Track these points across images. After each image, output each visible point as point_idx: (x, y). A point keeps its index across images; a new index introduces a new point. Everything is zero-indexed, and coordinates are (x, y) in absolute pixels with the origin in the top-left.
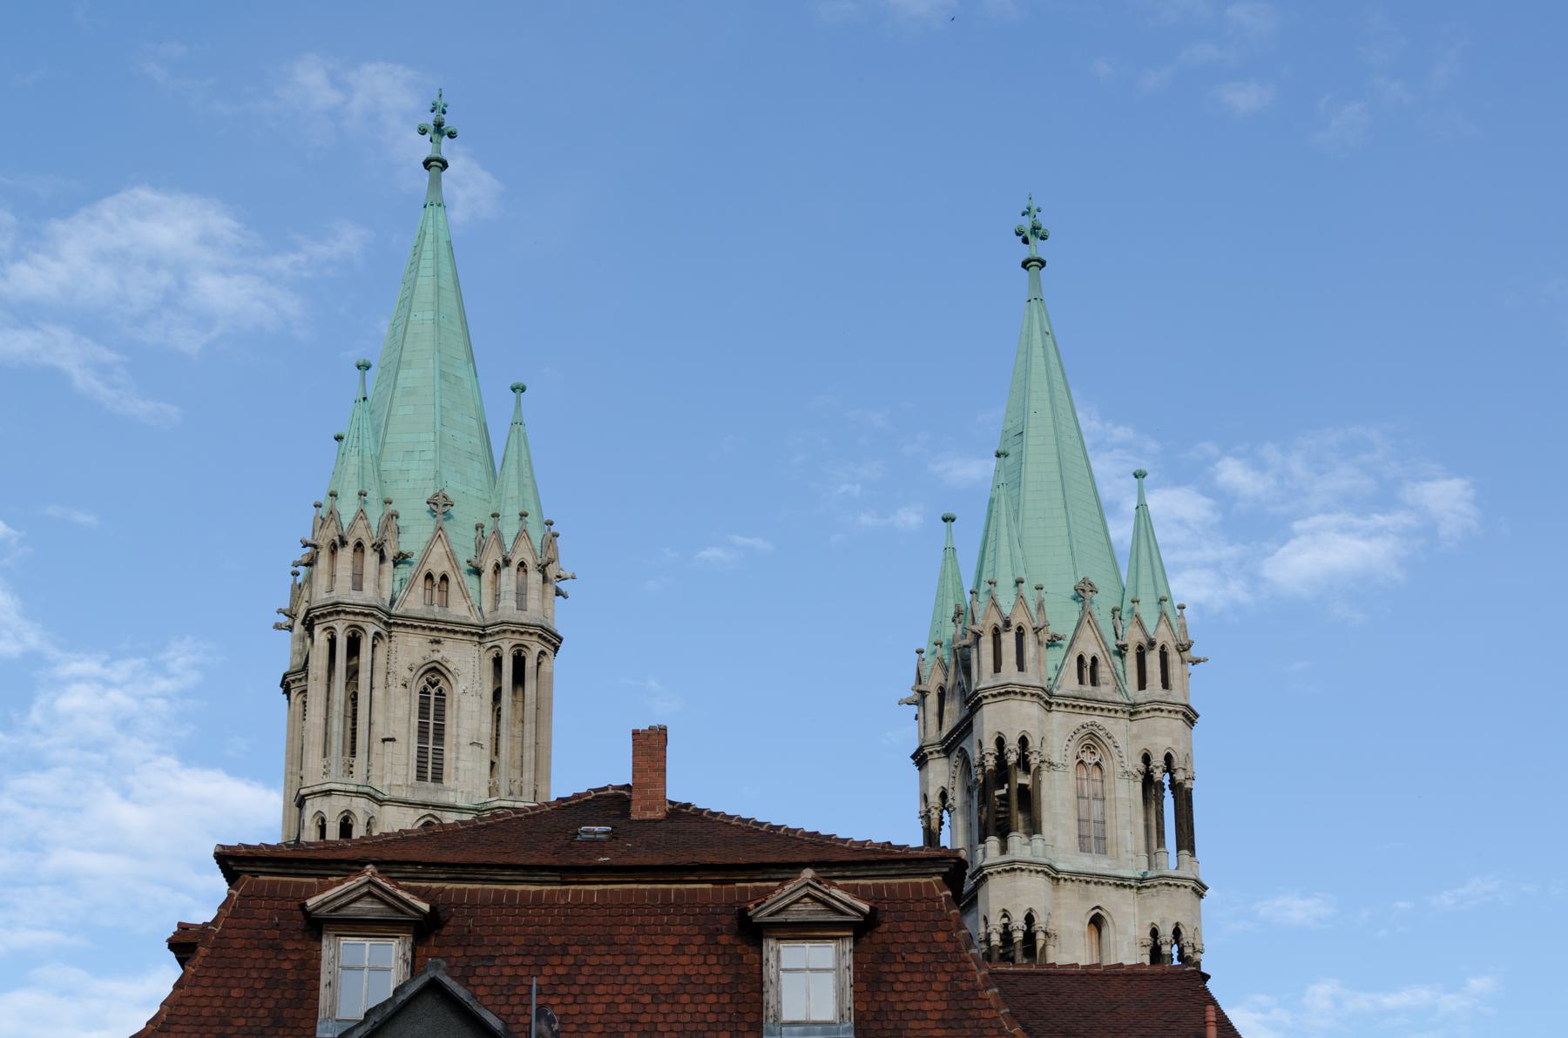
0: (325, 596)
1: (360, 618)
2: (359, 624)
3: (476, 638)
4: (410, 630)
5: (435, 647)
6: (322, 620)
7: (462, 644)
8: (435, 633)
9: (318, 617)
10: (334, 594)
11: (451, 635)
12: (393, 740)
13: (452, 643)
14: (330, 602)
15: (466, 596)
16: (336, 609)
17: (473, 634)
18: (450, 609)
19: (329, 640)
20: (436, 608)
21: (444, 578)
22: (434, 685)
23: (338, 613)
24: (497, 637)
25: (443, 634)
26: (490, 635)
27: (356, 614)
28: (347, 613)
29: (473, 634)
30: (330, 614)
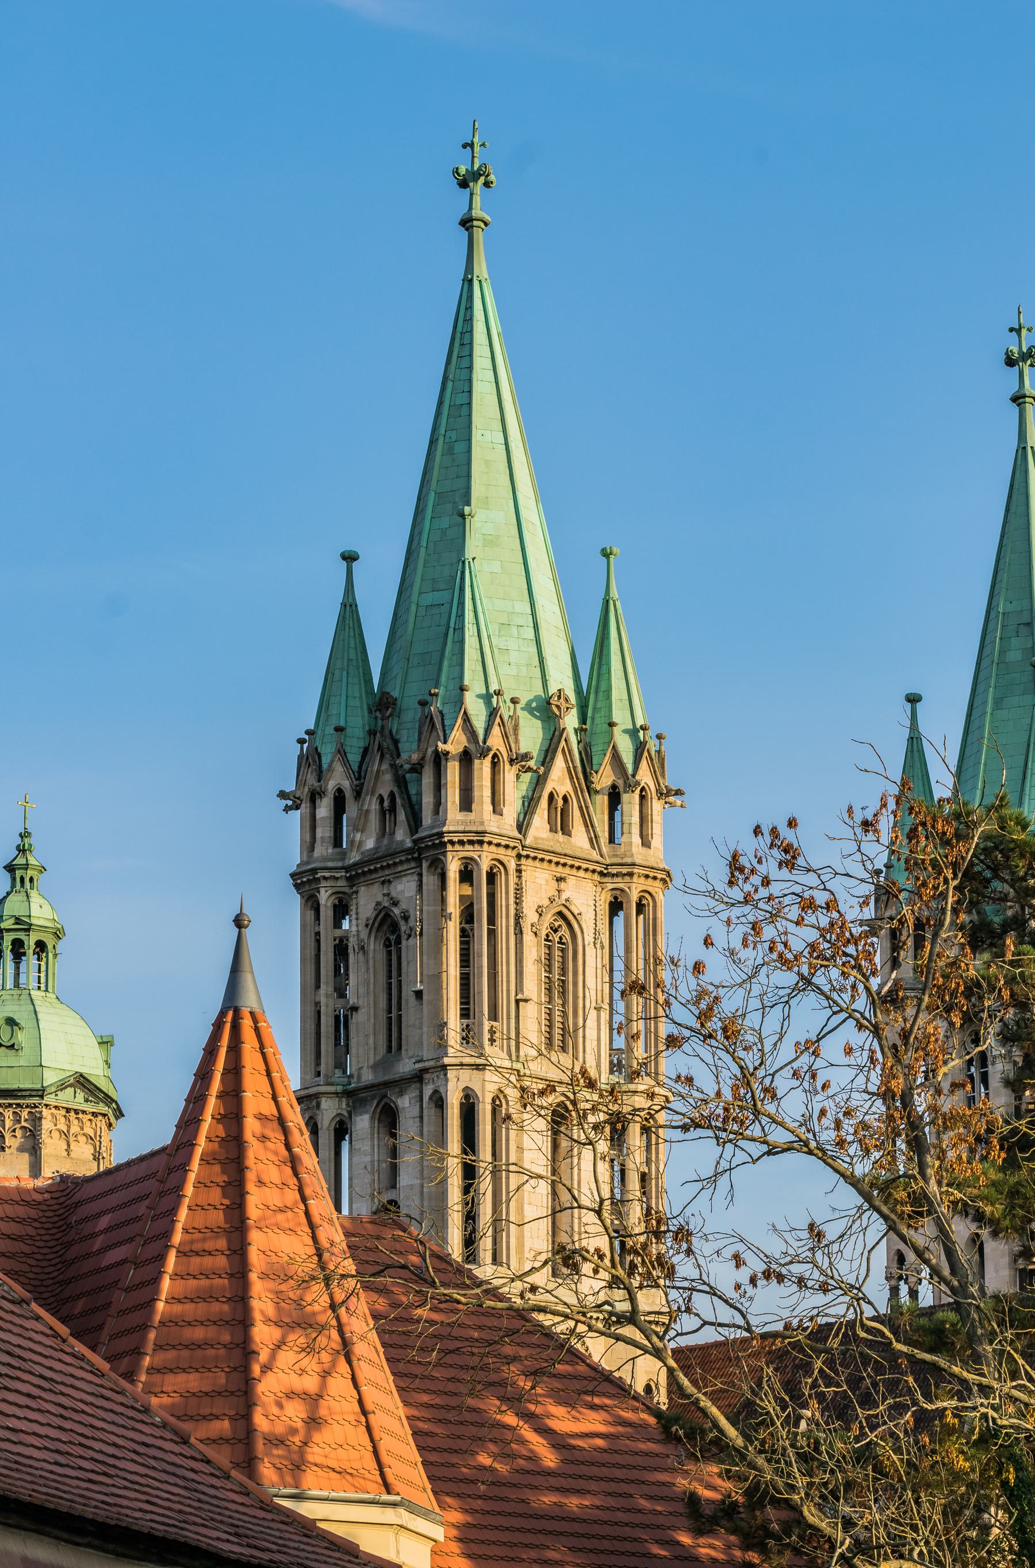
0: (461, 816)
1: (502, 850)
2: (501, 857)
3: (596, 877)
4: (537, 863)
5: (563, 885)
6: (457, 847)
7: (584, 883)
8: (560, 868)
9: (452, 843)
10: (472, 816)
11: (574, 872)
12: (526, 1001)
13: (574, 882)
14: (474, 829)
15: (589, 824)
16: (479, 839)
17: (594, 871)
18: (573, 840)
19: (460, 871)
20: (560, 836)
21: (565, 799)
22: (556, 931)
23: (481, 843)
24: (619, 879)
25: (567, 870)
26: (613, 875)
27: (498, 845)
28: (490, 843)
29: (594, 871)
30: (471, 842)
